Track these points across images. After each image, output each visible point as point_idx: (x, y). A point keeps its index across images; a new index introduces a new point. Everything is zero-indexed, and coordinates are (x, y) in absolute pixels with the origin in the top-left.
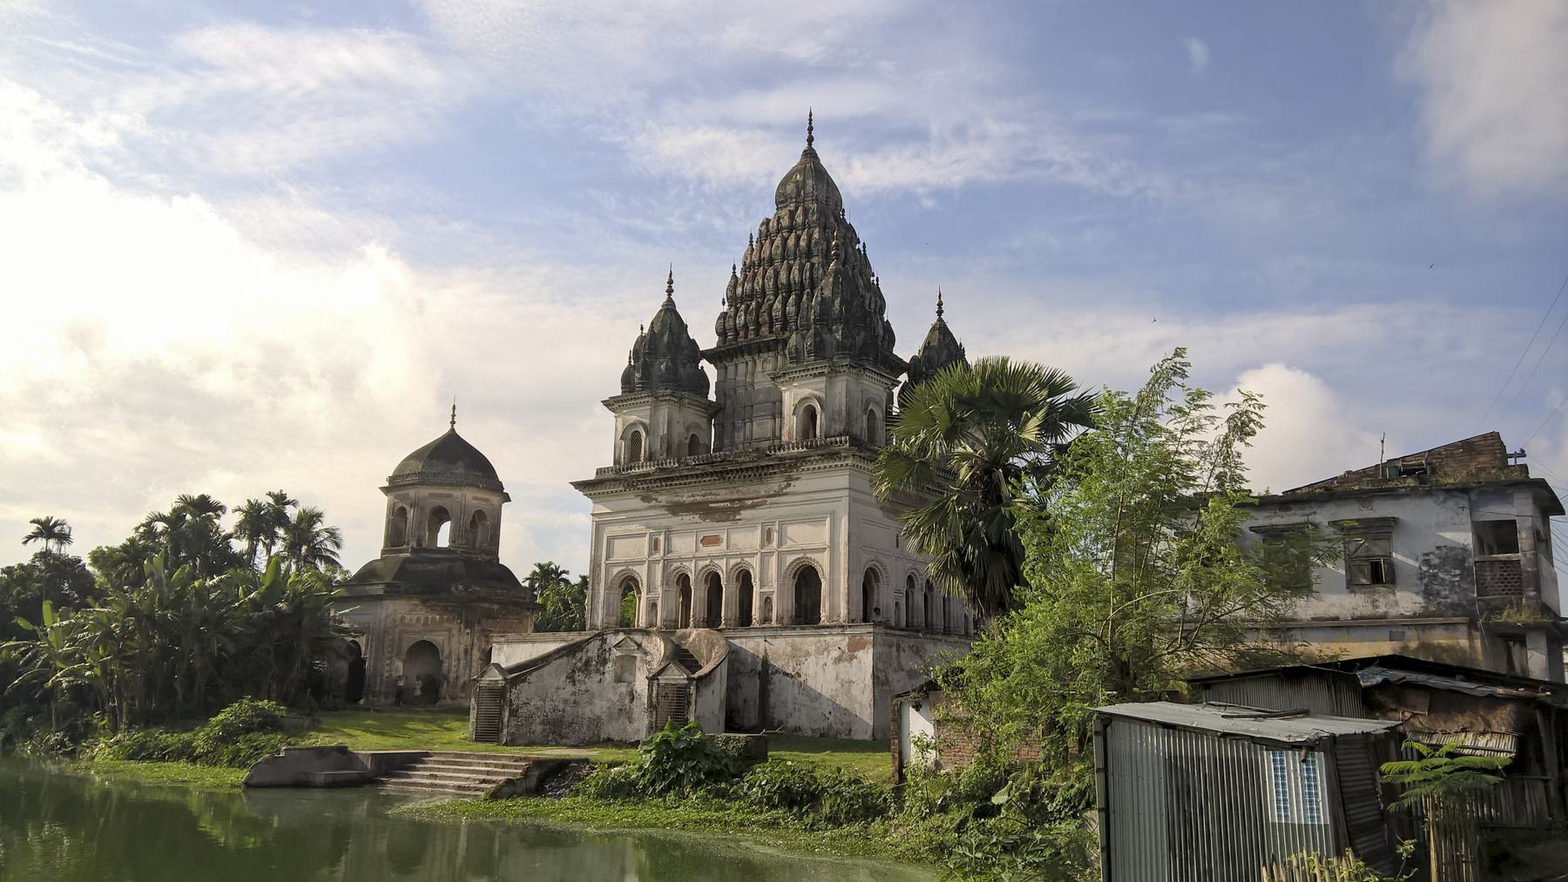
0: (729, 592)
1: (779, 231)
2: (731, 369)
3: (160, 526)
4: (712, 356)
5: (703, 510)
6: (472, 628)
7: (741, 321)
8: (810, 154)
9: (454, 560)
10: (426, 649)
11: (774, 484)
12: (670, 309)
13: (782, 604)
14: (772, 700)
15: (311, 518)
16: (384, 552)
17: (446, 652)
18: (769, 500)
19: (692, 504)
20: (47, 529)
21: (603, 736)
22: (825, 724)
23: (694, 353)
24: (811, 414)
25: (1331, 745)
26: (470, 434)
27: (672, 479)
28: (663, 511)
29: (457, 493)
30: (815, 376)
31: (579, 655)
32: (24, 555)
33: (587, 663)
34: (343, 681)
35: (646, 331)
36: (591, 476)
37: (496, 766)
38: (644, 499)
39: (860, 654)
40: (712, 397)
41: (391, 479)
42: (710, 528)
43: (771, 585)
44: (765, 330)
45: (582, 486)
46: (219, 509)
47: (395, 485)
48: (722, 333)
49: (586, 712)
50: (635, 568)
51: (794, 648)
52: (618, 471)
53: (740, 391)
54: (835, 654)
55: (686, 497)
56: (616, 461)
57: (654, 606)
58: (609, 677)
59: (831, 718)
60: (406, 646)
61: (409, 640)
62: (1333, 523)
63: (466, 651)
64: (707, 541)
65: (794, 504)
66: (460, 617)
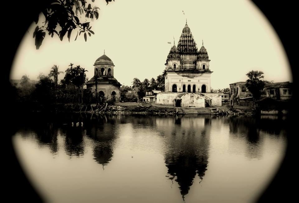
0: (192, 88)
2: (182, 56)
5: (188, 77)
7: (184, 49)
10: (114, 93)
11: (200, 74)
13: (201, 90)
21: (189, 106)
24: (204, 66)
38: (178, 74)
39: (220, 96)
43: (199, 87)
44: (188, 51)
50: (177, 84)
53: (184, 59)
55: (185, 75)
57: (180, 89)
61: (112, 91)
64: (189, 81)
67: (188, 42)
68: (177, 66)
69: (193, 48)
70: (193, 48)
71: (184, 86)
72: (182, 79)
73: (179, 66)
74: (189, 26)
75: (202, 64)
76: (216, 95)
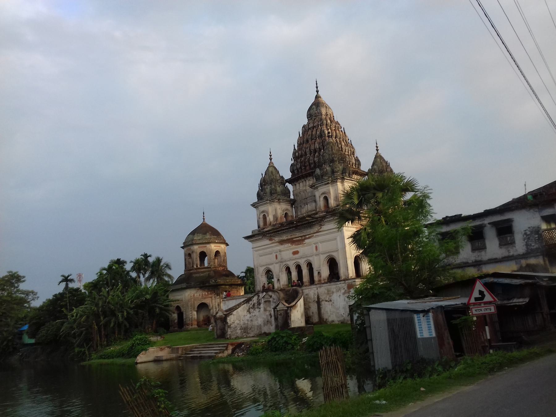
0: (305, 272)
1: (309, 129)
2: (297, 185)
3: (105, 272)
4: (290, 181)
5: (291, 241)
6: (219, 296)
7: (299, 166)
8: (317, 97)
9: (210, 271)
10: (203, 306)
11: (316, 229)
12: (271, 165)
14: (322, 311)
15: (159, 260)
16: (185, 271)
17: (211, 306)
18: (315, 235)
19: (287, 240)
20: (66, 279)
21: (263, 332)
22: (342, 318)
23: (283, 182)
24: (326, 199)
25: (436, 310)
26: (210, 222)
27: (279, 231)
28: (277, 244)
29: (208, 246)
30: (326, 184)
31: (250, 302)
32: (60, 289)
33: (254, 305)
34: (176, 321)
35: (263, 176)
36: (250, 234)
37: (222, 347)
38: (270, 240)
40: (292, 197)
41: (184, 243)
42: (295, 248)
44: (308, 168)
45: (247, 238)
46: (124, 262)
47: (187, 245)
48: (292, 171)
49: (256, 323)
51: (328, 291)
52: (259, 231)
53: (302, 193)
54: (343, 291)
55: (285, 237)
56: (259, 227)
57: (278, 280)
58: (262, 309)
59: (344, 316)
60: (197, 304)
62: (489, 224)
63: (218, 305)
65: (324, 235)
66: (214, 292)
67: (310, 142)
68: (270, 218)
69: (319, 154)
70: (319, 154)
71: (288, 270)
72: (280, 251)
73: (276, 218)
74: (325, 98)
75: (320, 197)
76: (340, 289)
